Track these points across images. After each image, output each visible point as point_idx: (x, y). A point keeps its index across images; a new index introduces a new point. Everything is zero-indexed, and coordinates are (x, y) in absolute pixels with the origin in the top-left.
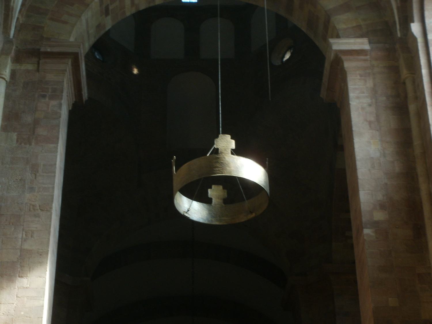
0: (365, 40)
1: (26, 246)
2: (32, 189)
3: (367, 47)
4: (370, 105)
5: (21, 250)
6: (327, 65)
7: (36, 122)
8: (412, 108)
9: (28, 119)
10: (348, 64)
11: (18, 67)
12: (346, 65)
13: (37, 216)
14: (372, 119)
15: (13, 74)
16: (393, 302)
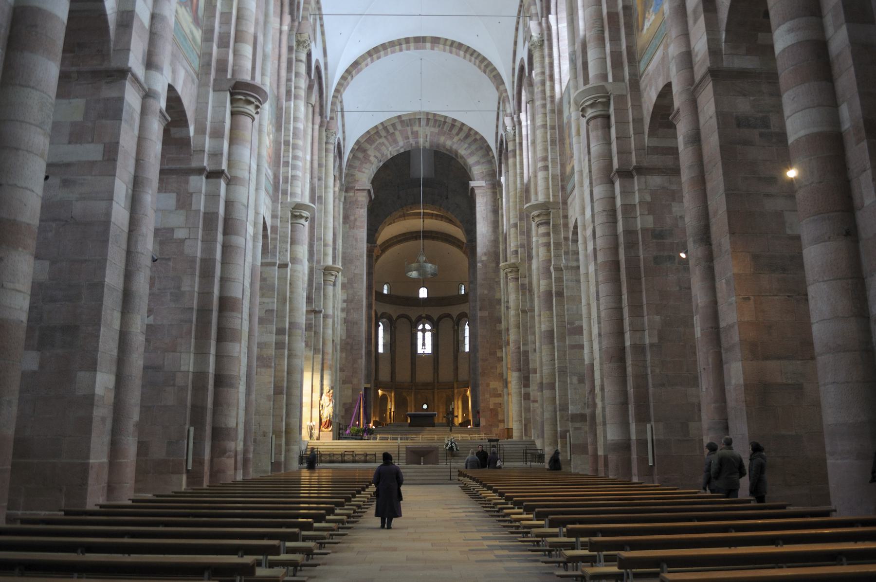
0: (484, 182)
1: (355, 272)
2: (356, 249)
3: (484, 185)
4: (484, 210)
5: (354, 274)
6: (470, 191)
7: (356, 220)
8: (500, 212)
9: (352, 218)
10: (477, 191)
11: (346, 194)
12: (476, 191)
13: (358, 259)
14: (485, 216)
15: (345, 197)
16: (486, 292)
